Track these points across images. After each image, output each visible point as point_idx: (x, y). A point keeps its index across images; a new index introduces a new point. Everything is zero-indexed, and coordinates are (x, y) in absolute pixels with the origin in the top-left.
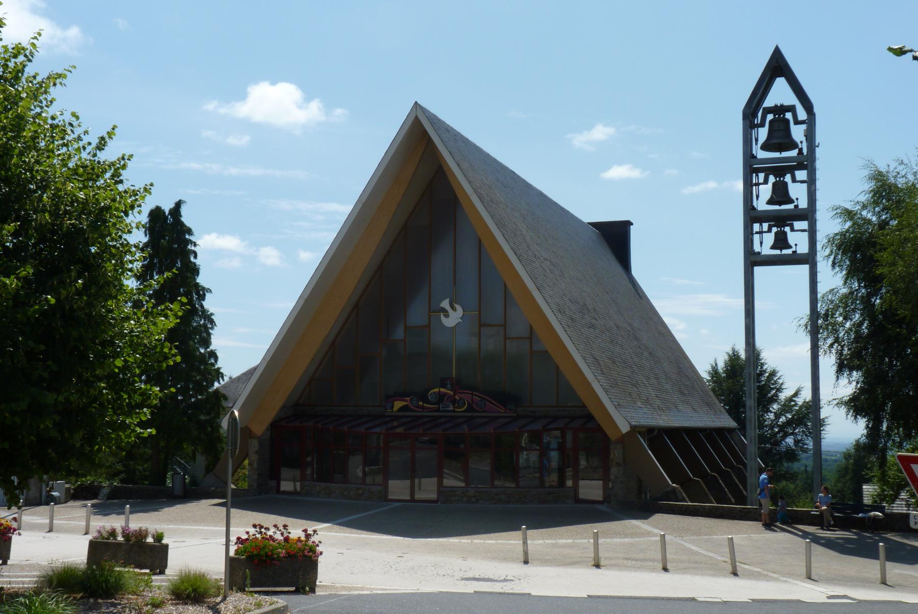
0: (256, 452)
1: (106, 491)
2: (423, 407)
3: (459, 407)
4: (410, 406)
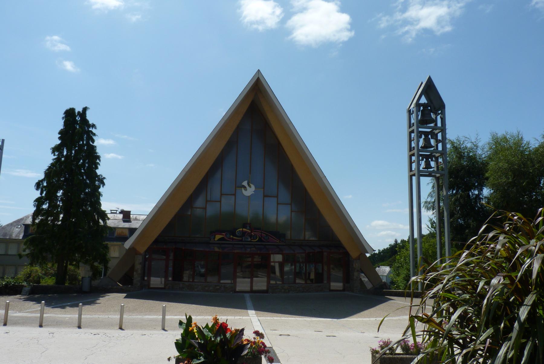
0: (140, 264)
1: (27, 289)
2: (233, 239)
3: (254, 239)
4: (225, 237)
